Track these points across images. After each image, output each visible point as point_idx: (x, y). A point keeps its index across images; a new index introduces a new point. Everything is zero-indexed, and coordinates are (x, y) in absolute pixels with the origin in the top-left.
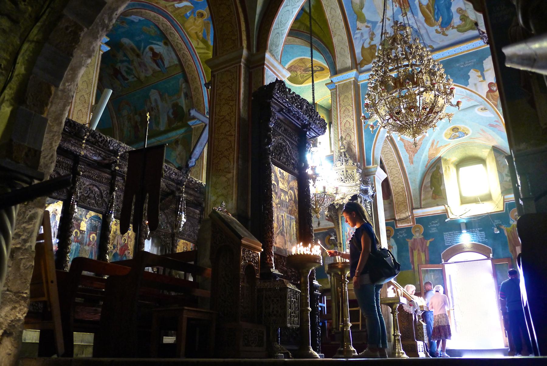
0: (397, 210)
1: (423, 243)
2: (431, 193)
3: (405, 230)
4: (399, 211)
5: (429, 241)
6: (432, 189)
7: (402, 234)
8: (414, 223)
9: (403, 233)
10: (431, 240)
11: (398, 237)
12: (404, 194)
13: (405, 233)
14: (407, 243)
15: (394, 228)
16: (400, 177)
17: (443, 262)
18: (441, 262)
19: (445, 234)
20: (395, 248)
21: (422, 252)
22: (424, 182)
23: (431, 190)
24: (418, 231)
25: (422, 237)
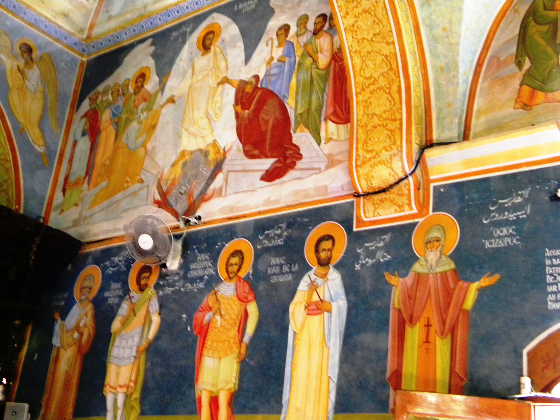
0: (361, 152)
1: (448, 294)
2: (516, 82)
3: (387, 237)
4: (368, 156)
5: (474, 287)
6: (520, 65)
7: (371, 254)
8: (422, 207)
9: (377, 249)
10: (485, 282)
11: (358, 267)
12: (395, 88)
13: (387, 248)
16: (379, 11)
17: (527, 390)
18: (518, 388)
19: (551, 258)
20: (339, 308)
21: (442, 334)
22: (493, 43)
23: (516, 69)
24: (438, 240)
25: (449, 266)
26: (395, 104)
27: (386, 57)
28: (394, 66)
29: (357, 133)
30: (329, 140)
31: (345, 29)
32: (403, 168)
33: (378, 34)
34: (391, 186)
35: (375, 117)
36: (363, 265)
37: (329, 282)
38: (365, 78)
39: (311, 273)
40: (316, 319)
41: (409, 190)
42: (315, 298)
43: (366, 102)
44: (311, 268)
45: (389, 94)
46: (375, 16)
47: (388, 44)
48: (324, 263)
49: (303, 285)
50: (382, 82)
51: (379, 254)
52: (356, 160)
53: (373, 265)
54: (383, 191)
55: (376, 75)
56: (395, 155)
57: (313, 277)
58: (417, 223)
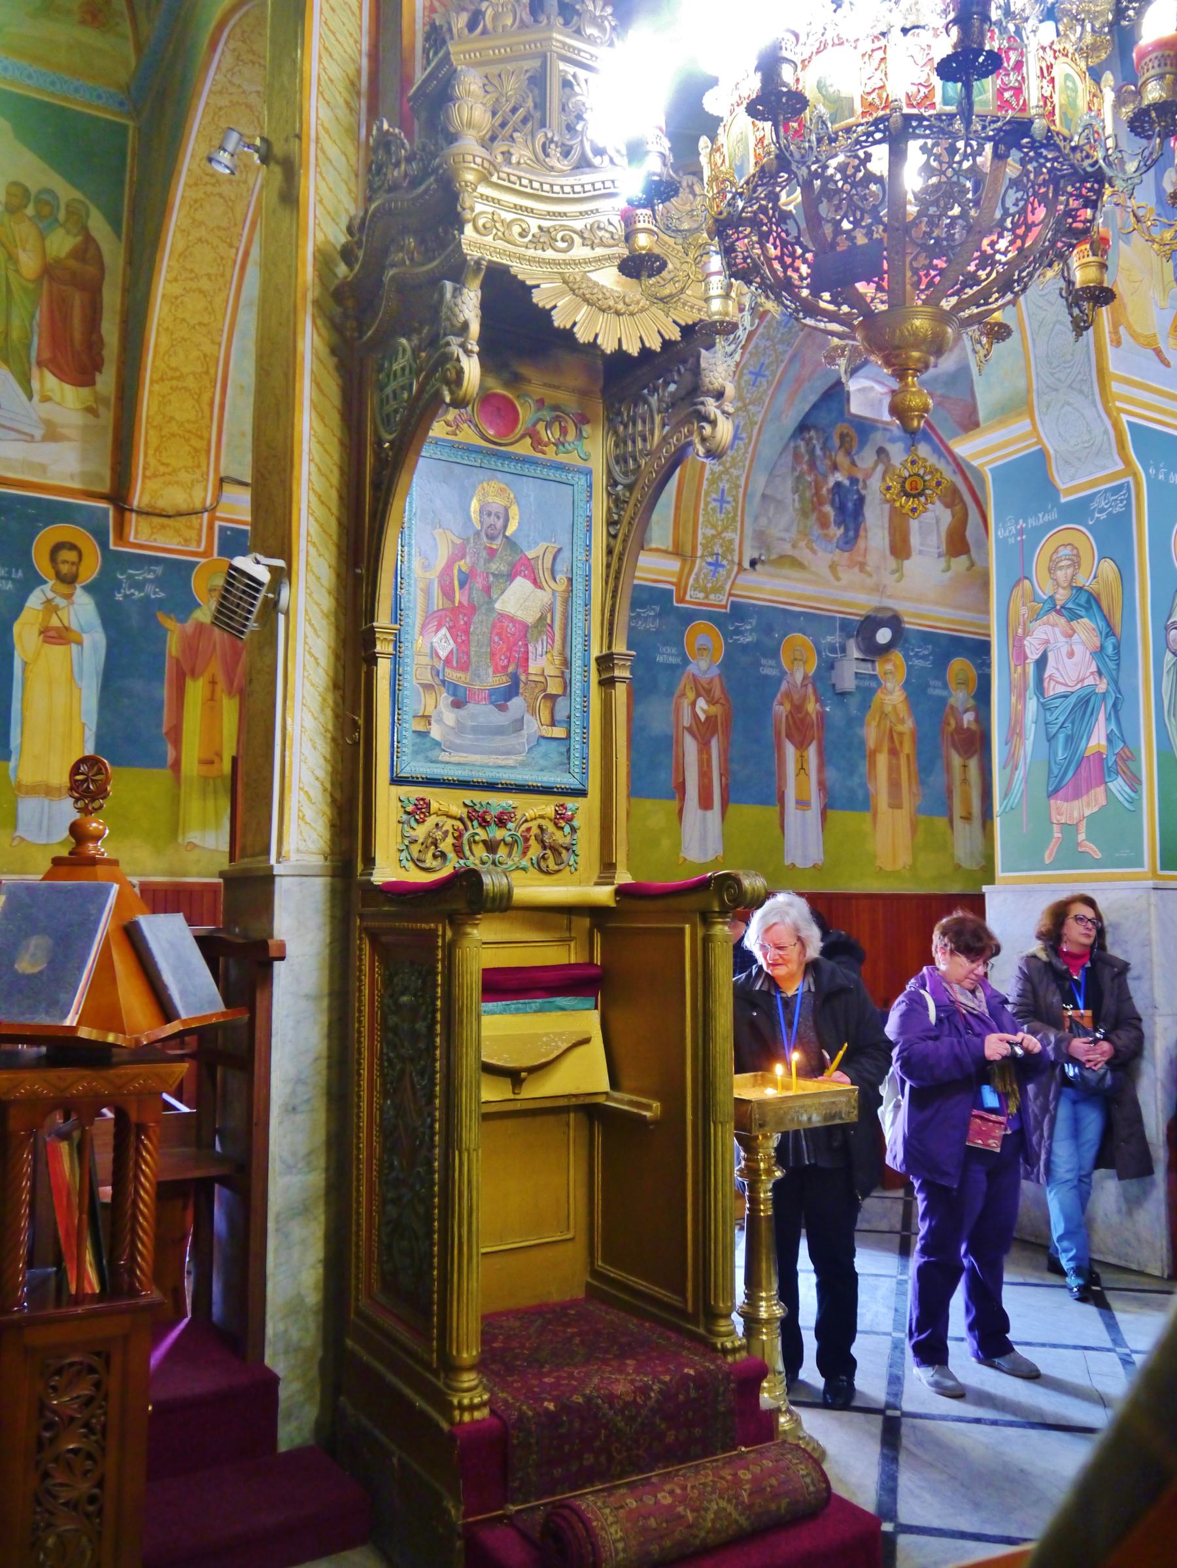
0: (152, 461)
3: (159, 570)
4: (162, 469)
7: (140, 586)
9: (146, 581)
11: (119, 597)
12: (206, 397)
13: (159, 582)
14: (160, 637)
15: (104, 545)
16: (218, 301)
21: (230, 693)
26: (203, 417)
27: (205, 356)
28: (212, 371)
29: (147, 433)
30: (46, 399)
31: (163, 296)
32: (205, 500)
33: (205, 325)
34: (180, 514)
35: (174, 423)
36: (126, 596)
37: (75, 606)
38: (168, 366)
39: (47, 588)
40: (57, 652)
41: (201, 525)
42: (55, 622)
43: (164, 397)
44: (45, 582)
45: (198, 401)
46: (211, 302)
47: (213, 342)
48: (69, 580)
49: (35, 600)
50: (191, 383)
51: (149, 588)
52: (145, 469)
53: (141, 599)
54: (169, 517)
55: (185, 370)
56: (198, 481)
57: (50, 595)
58: (198, 563)
